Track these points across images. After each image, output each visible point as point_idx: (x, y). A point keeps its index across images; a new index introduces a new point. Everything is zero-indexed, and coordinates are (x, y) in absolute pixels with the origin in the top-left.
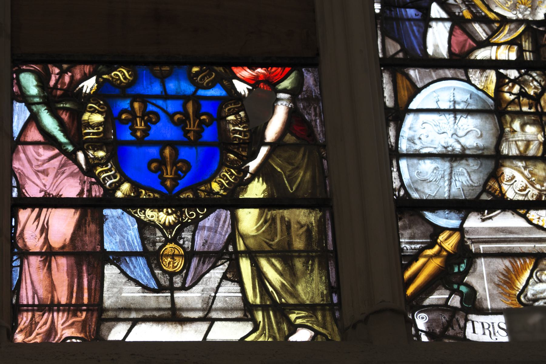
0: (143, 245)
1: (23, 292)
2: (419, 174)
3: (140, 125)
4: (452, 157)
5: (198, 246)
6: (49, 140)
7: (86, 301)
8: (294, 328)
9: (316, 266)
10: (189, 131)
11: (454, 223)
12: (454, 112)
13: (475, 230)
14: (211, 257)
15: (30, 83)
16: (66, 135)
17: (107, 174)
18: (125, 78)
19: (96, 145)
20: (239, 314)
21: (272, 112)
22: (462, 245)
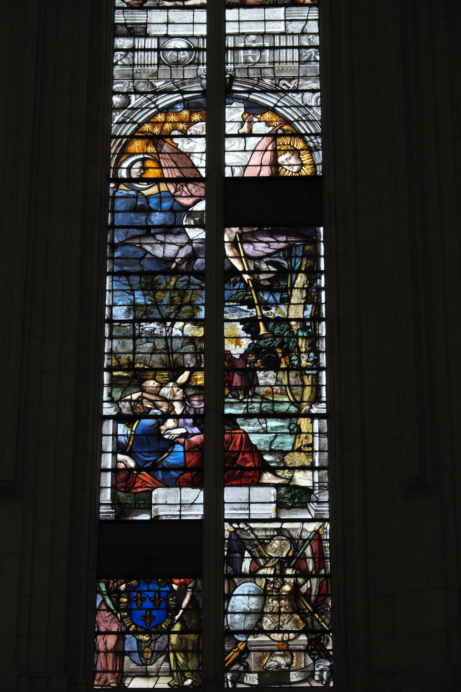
0: (138, 648)
1: (98, 666)
2: (234, 620)
3: (139, 602)
4: (246, 613)
5: (156, 649)
6: (109, 609)
7: (118, 669)
8: (186, 679)
9: (195, 656)
10: (156, 605)
11: (244, 639)
12: (249, 595)
13: (251, 641)
14: (160, 653)
15: (103, 587)
16: (114, 607)
17: (127, 622)
18: (135, 584)
19: (124, 610)
20: (168, 674)
21: (185, 596)
22: (246, 647)
